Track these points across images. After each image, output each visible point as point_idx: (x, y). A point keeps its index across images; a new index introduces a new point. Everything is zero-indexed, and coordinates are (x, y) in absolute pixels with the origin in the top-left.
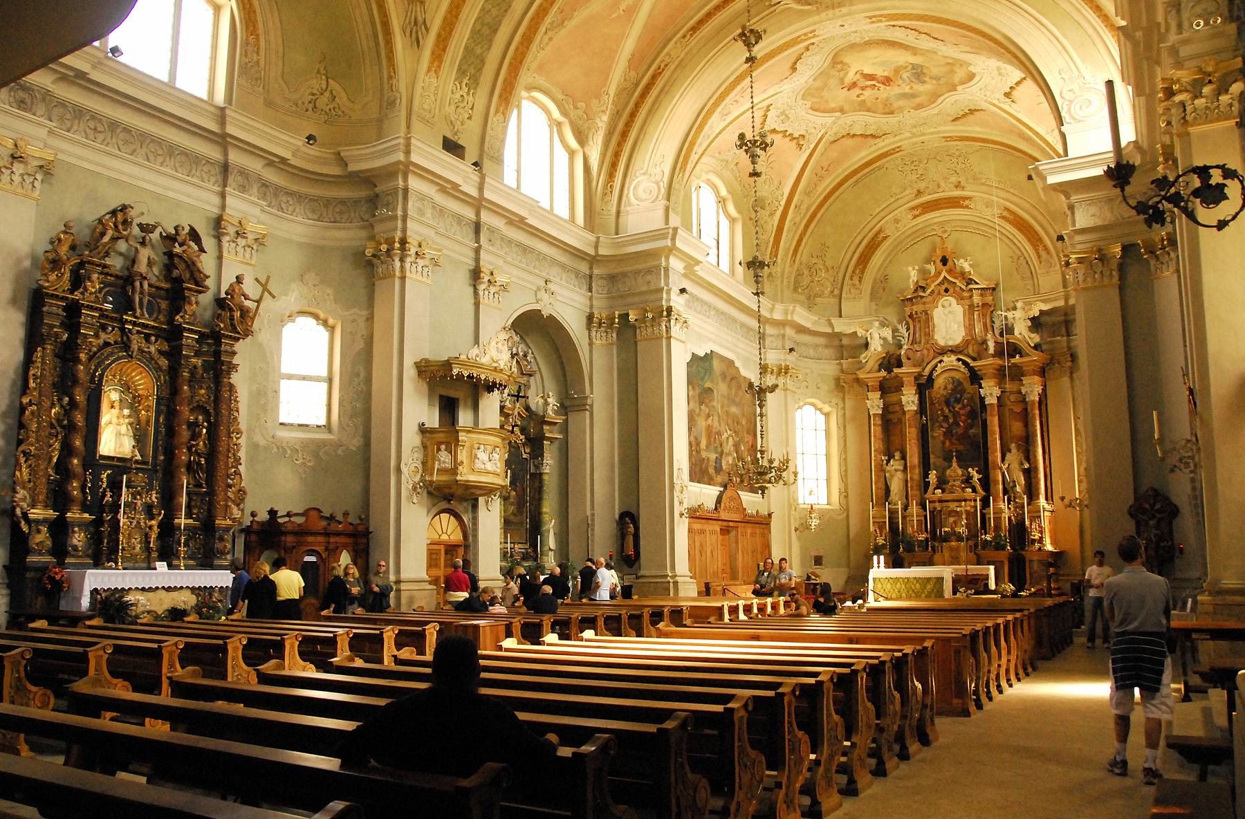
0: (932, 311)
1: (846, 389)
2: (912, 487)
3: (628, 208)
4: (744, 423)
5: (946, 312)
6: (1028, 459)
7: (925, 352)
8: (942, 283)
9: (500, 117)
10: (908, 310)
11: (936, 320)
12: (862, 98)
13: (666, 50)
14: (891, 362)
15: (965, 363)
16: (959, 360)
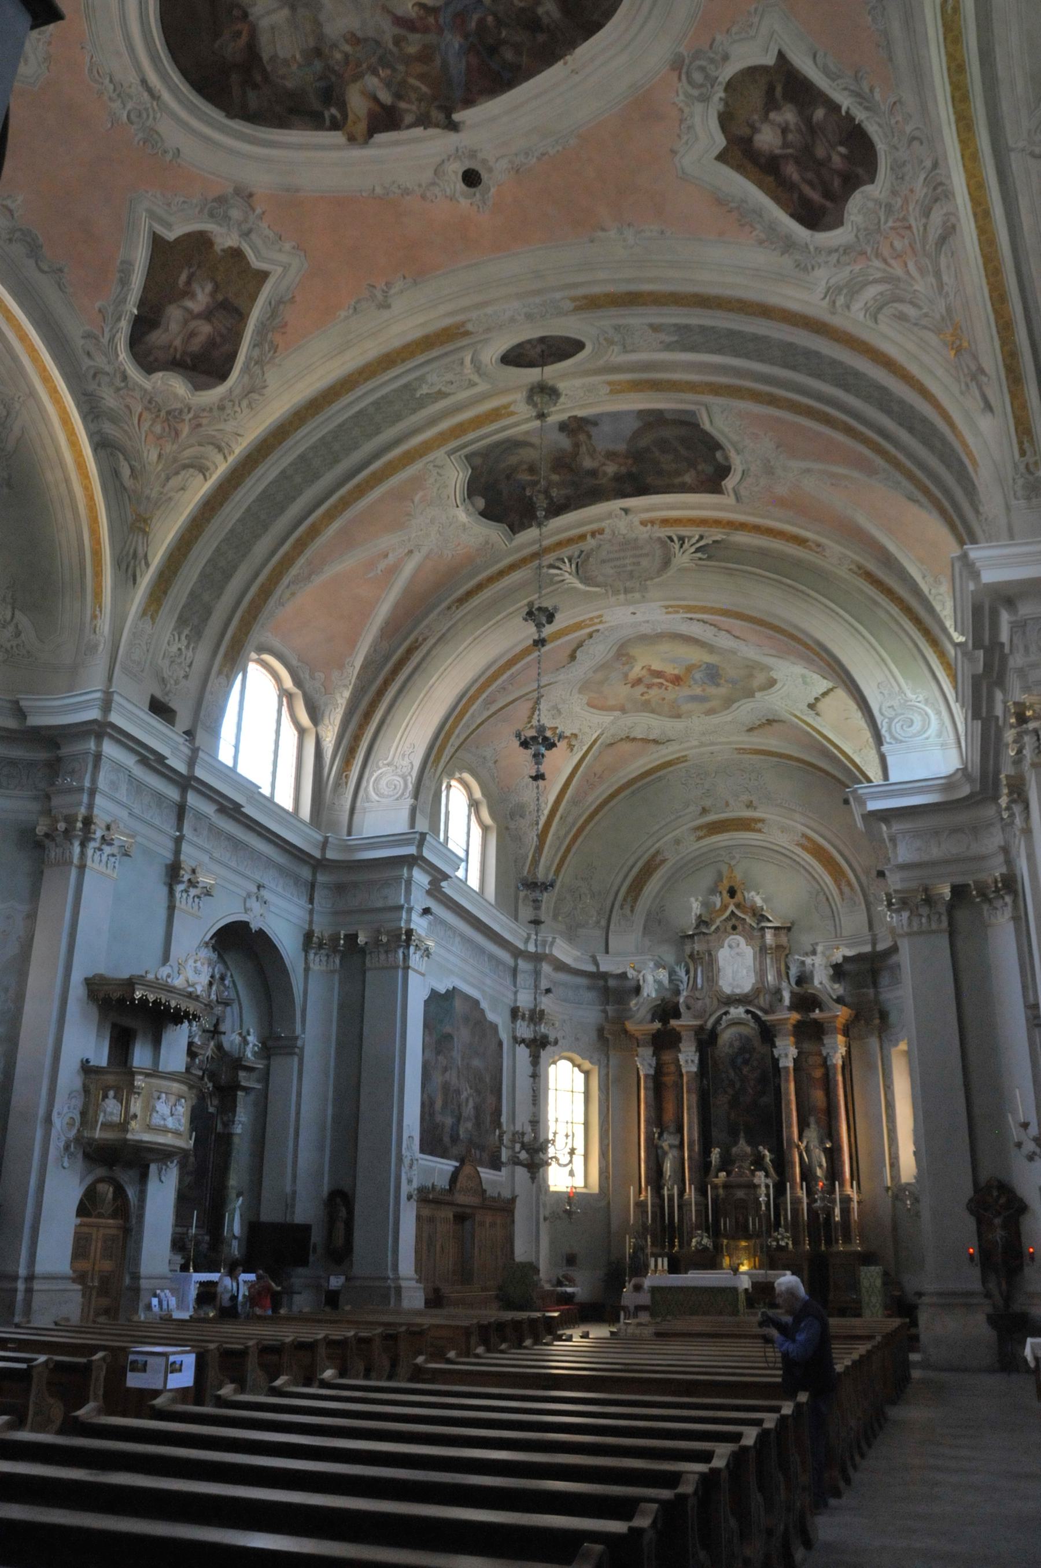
0: (717, 951)
3: (366, 805)
4: (488, 1080)
7: (708, 1001)
8: (728, 919)
9: (222, 679)
10: (688, 949)
11: (721, 963)
12: (646, 697)
13: (425, 623)
14: (666, 1011)
15: (755, 1016)
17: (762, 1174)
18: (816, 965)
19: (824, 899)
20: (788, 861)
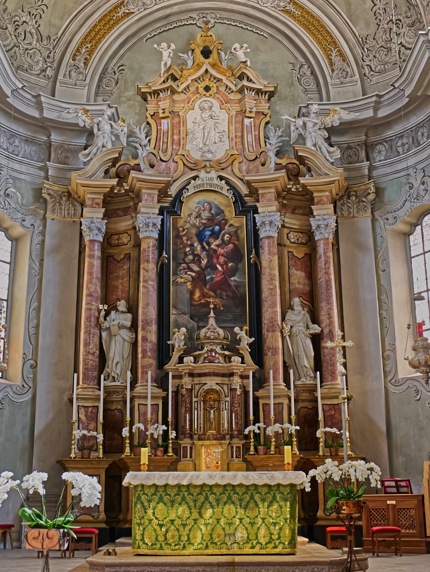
0: (186, 113)
1: (50, 206)
2: (144, 352)
5: (206, 115)
6: (315, 320)
7: (172, 165)
11: (190, 125)
16: (221, 178)
17: (236, 359)
18: (309, 125)
19: (309, 73)
20: (270, 31)
